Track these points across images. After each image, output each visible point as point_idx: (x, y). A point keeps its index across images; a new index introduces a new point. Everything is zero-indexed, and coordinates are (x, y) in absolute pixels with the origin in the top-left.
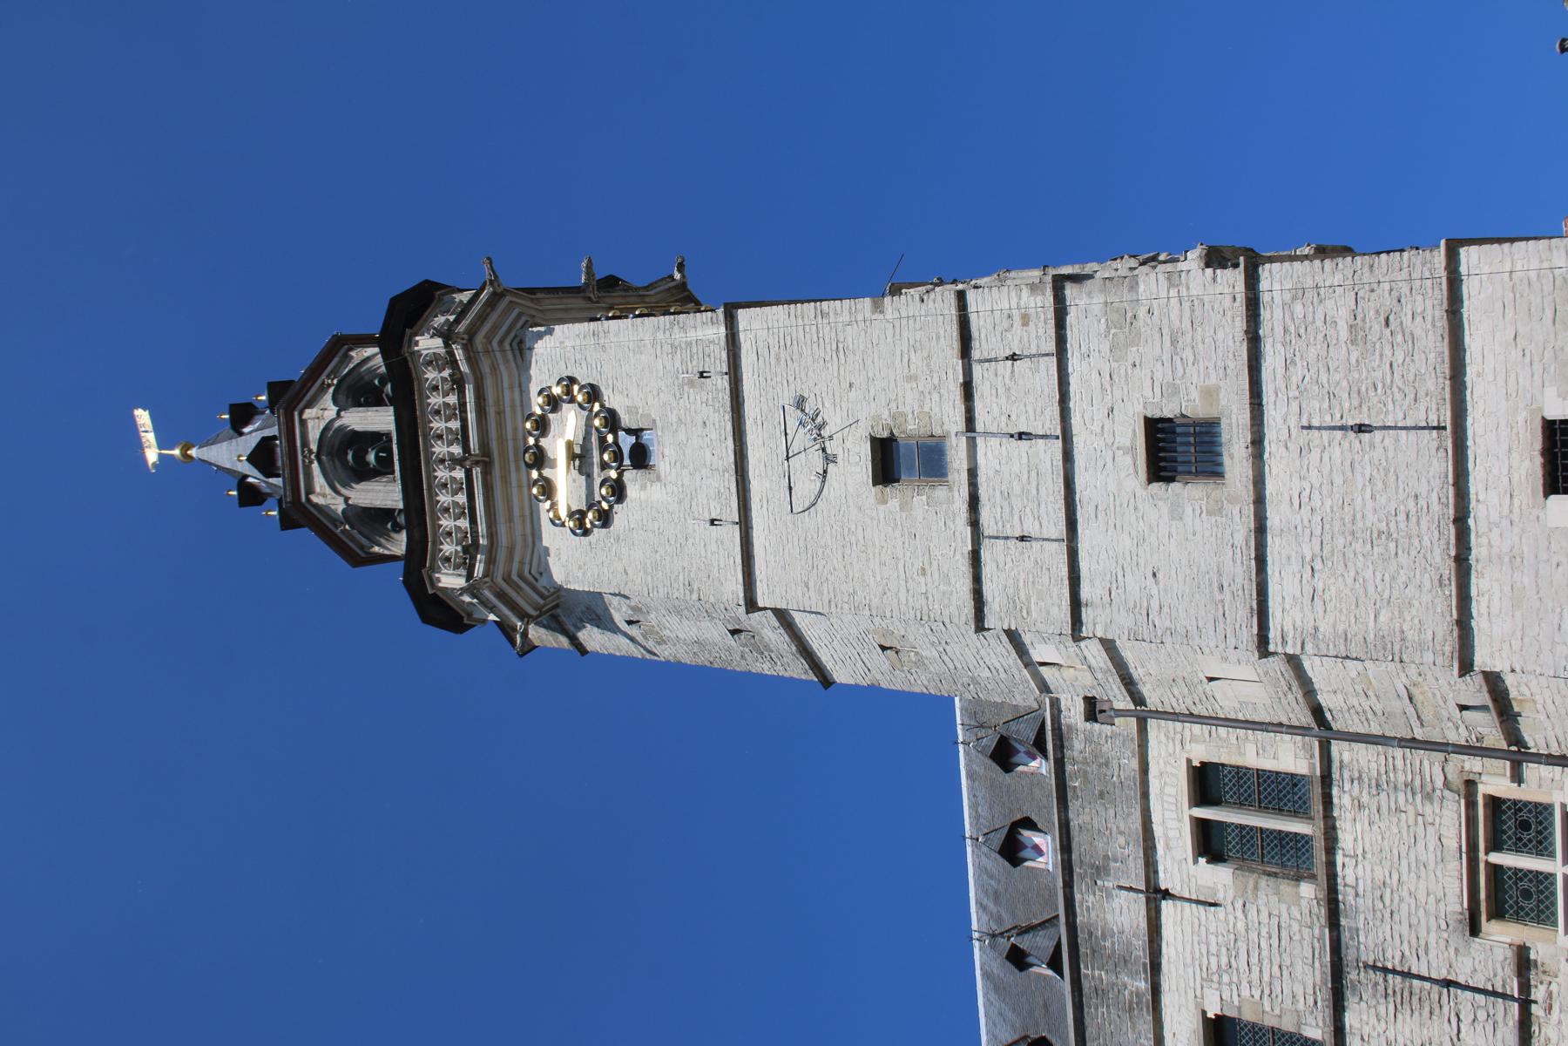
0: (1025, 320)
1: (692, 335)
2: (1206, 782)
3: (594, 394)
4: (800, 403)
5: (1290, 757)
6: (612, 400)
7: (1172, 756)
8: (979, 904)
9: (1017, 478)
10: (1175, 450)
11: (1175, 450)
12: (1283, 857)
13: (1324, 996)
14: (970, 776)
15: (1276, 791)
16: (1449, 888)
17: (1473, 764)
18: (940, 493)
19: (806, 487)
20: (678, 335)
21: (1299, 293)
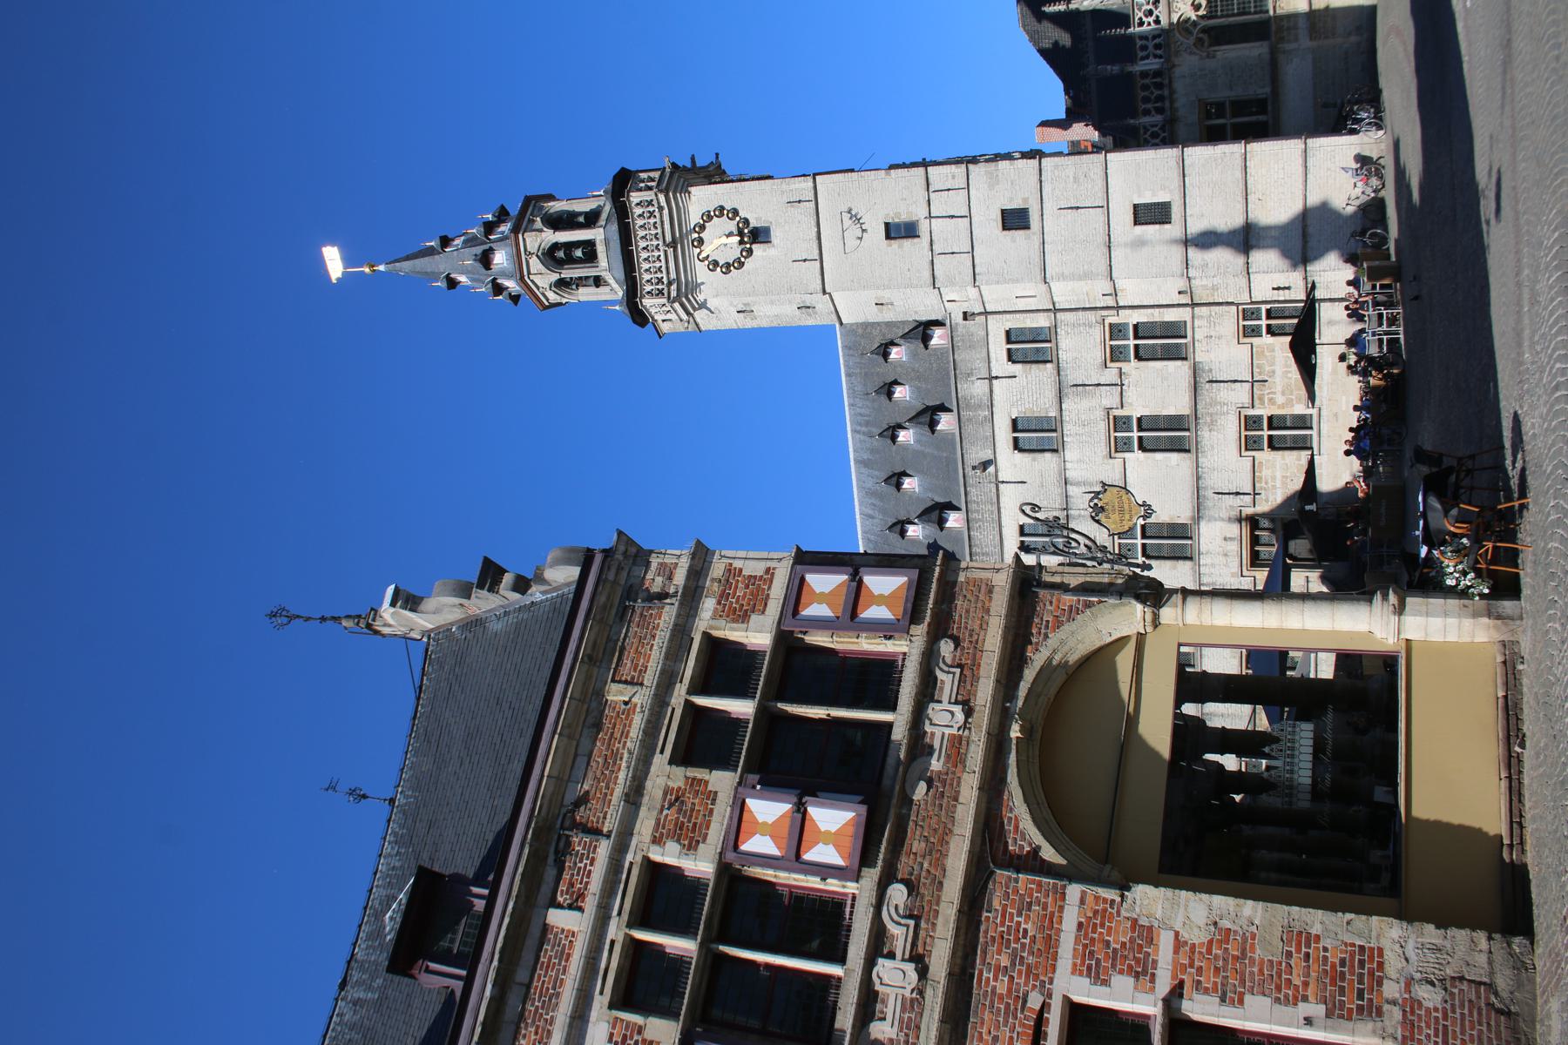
2: (1009, 336)
3: (735, 212)
5: (1042, 321)
6: (742, 214)
7: (997, 327)
8: (854, 431)
9: (947, 234)
10: (1014, 220)
11: (1014, 220)
12: (1039, 359)
13: (1055, 401)
14: (848, 375)
15: (1036, 336)
16: (1097, 354)
17: (1105, 313)
19: (851, 242)
21: (1056, 167)
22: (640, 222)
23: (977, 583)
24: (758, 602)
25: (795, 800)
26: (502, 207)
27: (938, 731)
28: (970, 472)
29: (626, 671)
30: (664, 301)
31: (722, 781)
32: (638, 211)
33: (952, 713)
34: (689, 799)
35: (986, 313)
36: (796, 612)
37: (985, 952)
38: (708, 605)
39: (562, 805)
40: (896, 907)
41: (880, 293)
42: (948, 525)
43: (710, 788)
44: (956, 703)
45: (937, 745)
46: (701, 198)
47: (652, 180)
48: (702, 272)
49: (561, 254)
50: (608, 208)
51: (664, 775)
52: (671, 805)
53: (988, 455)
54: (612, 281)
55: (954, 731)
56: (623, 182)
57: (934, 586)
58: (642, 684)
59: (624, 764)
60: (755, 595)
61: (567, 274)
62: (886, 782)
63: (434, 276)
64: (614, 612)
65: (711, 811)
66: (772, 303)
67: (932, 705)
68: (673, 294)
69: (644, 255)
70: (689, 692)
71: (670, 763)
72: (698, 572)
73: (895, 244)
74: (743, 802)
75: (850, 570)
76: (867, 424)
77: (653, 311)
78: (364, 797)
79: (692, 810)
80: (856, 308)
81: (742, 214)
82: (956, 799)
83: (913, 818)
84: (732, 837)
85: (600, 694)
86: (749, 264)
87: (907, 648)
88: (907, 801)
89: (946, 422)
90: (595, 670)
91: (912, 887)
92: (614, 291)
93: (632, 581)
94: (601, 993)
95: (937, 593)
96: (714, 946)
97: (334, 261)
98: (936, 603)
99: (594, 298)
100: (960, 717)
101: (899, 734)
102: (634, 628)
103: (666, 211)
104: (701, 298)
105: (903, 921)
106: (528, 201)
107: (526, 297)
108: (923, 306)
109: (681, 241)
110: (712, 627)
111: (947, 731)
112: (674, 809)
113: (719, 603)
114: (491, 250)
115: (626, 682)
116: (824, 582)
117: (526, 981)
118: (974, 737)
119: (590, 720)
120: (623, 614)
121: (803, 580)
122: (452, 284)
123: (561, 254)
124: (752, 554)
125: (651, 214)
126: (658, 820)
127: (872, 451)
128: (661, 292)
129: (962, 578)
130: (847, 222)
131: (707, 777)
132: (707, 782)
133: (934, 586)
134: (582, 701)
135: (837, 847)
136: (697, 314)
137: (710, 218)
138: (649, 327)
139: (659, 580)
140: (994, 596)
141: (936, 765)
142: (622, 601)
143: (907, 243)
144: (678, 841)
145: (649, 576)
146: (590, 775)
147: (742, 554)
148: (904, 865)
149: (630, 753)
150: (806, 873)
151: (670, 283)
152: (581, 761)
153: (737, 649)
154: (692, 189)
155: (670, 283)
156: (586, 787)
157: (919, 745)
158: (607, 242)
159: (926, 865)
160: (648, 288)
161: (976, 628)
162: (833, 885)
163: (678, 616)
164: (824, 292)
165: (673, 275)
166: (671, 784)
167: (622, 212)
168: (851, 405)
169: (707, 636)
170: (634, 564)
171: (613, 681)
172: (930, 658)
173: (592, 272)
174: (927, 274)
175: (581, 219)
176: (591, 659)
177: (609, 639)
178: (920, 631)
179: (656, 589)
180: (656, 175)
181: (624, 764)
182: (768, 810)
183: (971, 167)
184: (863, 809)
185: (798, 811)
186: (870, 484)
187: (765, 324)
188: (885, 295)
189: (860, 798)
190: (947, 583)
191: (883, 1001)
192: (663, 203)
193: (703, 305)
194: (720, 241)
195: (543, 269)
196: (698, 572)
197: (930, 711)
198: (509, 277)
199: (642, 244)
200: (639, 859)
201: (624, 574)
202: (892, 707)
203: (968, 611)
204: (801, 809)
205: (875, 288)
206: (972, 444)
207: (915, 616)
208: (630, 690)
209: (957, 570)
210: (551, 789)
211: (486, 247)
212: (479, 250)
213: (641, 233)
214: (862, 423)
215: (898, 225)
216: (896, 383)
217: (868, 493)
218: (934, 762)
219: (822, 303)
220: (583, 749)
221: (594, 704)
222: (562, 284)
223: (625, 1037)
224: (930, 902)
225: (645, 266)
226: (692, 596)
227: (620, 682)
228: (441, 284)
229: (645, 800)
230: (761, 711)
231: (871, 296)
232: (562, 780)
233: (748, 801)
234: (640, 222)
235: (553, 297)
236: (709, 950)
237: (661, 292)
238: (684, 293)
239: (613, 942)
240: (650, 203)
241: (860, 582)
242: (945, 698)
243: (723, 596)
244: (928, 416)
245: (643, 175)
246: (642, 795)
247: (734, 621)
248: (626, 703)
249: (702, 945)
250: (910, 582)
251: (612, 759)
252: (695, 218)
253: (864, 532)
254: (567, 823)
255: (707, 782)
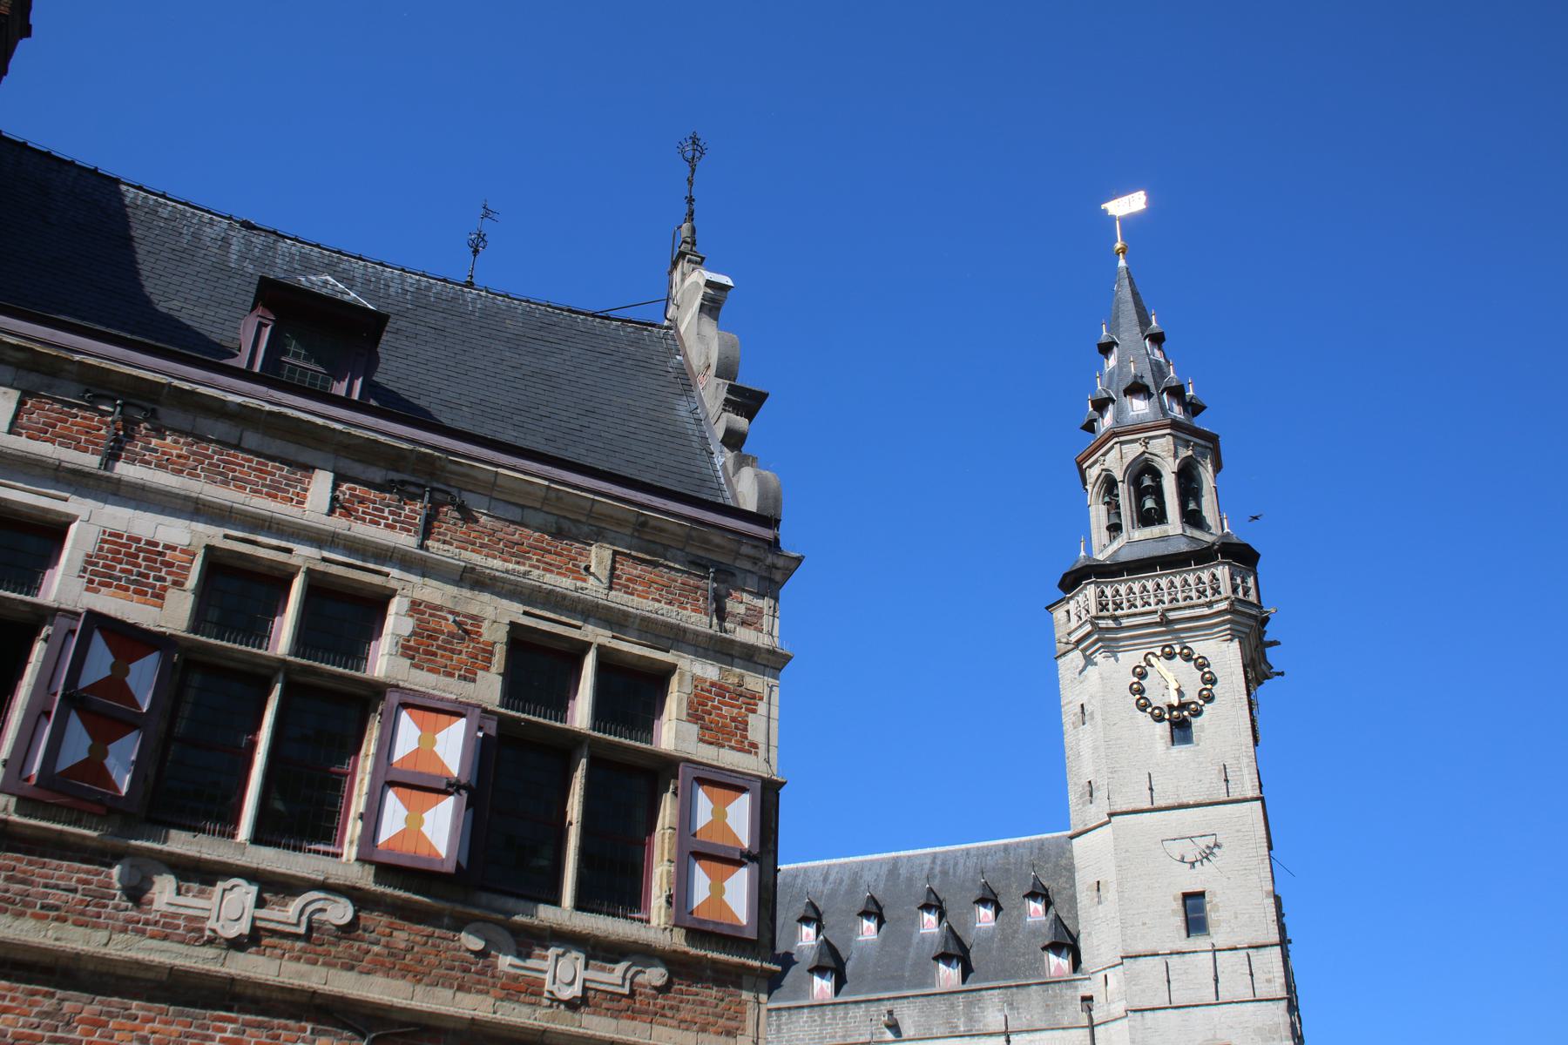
0: (1269, 981)
1: (1246, 771)
3: (1209, 699)
4: (1217, 845)
6: (1207, 708)
8: (935, 856)
9: (1193, 975)
14: (1006, 847)
18: (1183, 933)
19: (1177, 849)
20: (1245, 761)
22: (1191, 579)
23: (739, 1015)
24: (714, 734)
25: (464, 781)
26: (1203, 408)
27: (547, 965)
28: (887, 1006)
29: (627, 569)
30: (1093, 612)
31: (488, 688)
32: (1206, 576)
33: (571, 983)
34: (466, 648)
35: (1092, 1027)
36: (701, 781)
37: (259, 1026)
38: (710, 671)
39: (461, 489)
40: (322, 910)
41: (1113, 888)
42: (816, 979)
43: (480, 673)
44: (585, 989)
45: (530, 963)
46: (1225, 656)
47: (1246, 593)
48: (1131, 658)
49: (1147, 481)
50: (1208, 538)
51: (498, 616)
52: (458, 624)
53: (908, 1029)
54: (1115, 546)
55: (548, 986)
56: (1242, 556)
57: (736, 959)
58: (610, 588)
59: (511, 566)
60: (722, 729)
61: (1124, 492)
62: (484, 898)
63: (1114, 327)
64: (701, 553)
65: (452, 675)
66: (1095, 749)
67: (582, 957)
68: (1103, 624)
69: (1150, 585)
70: (600, 648)
71: (512, 624)
72: (750, 657)
73: (1178, 905)
74: (461, 715)
75: (756, 851)
76: (944, 873)
77: (1080, 598)
78: (476, 252)
79: (453, 651)
80: (1093, 856)
81: (1207, 708)
82: (460, 988)
83: (438, 932)
84: (418, 701)
85: (599, 536)
86: (1144, 718)
87: (655, 924)
88: (459, 924)
89: (948, 975)
90: (628, 531)
91: (348, 930)
92: (1103, 549)
93: (740, 576)
94: (226, 537)
95: (727, 963)
96: (281, 677)
97: (1128, 205)
98: (714, 962)
99: (1093, 520)
100: (567, 994)
101: (546, 914)
102: (680, 578)
103: (1206, 611)
104: (1099, 658)
105: (304, 919)
106: (1213, 439)
107: (1091, 440)
108: (1098, 943)
109: (1170, 632)
110: (682, 675)
111: (548, 977)
112: (455, 629)
113: (713, 684)
114: (1149, 395)
115: (613, 568)
116: (739, 816)
117: (244, 445)
118: (540, 1012)
119: (566, 525)
120: (698, 565)
121: (742, 790)
122: (1106, 349)
123: (1147, 481)
124: (774, 725)
125: (1202, 593)
126: (440, 608)
127: (910, 880)
128: (1104, 607)
129: (746, 995)
130: (1203, 843)
131: (494, 669)
132: (487, 669)
133: (736, 959)
134: (590, 514)
135: (403, 833)
136: (1077, 654)
137: (1200, 667)
138: (1061, 594)
139: (741, 609)
140: (723, 1039)
141: (505, 962)
142: (714, 563)
143: (1179, 921)
144: (414, 633)
145: (746, 597)
146: (499, 524)
147: (775, 712)
148: (377, 921)
149: (526, 574)
150: (371, 794)
151: (1115, 618)
152: (515, 513)
153: (654, 707)
154: (1236, 644)
155: (1115, 618)
156: (483, 519)
157: (530, 940)
158: (1164, 538)
159: (376, 949)
160: (1109, 591)
161: (682, 1015)
162: (354, 829)
163: (697, 634)
164: (1111, 815)
165: (1125, 622)
166: (486, 624)
167: (1203, 556)
168: (968, 852)
169: (671, 669)
170: (761, 578)
171: (615, 553)
172: (643, 954)
173: (1126, 520)
174: (1140, 948)
175: (1192, 506)
176: (642, 525)
177: (667, 547)
178: (677, 941)
179: (731, 605)
180: (1252, 598)
181: (511, 566)
182: (451, 747)
183: (1284, 1004)
184: (450, 868)
185: (450, 785)
186: (868, 877)
187: (1069, 739)
188: (1110, 894)
189: (464, 863)
190: (739, 976)
191: (201, 892)
192: (1216, 608)
193: (1089, 661)
194: (1171, 680)
195: (1127, 461)
196: (750, 657)
197: (574, 954)
198: (1117, 419)
199: (1164, 583)
200: (393, 584)
201: (748, 566)
202: (581, 905)
203: (703, 1003)
204: (451, 788)
205: (1119, 879)
206: (921, 1010)
207: (698, 934)
208: (604, 574)
209: (756, 989)
210: (481, 476)
211: (1153, 389)
212: (1149, 380)
213: (1178, 581)
214: (945, 866)
215: (1201, 909)
216: (998, 909)
217: (856, 875)
218: (509, 959)
219: (1097, 812)
220: (530, 516)
221: (586, 529)
222: (1110, 484)
223: (170, 565)
224: (328, 953)
225: (1136, 587)
226: (721, 650)
227: (614, 561)
228: (1105, 336)
229: (466, 593)
230: (577, 738)
231: (1109, 877)
232: (492, 489)
233: (463, 721)
234: (1191, 579)
235: (1093, 473)
236: (276, 671)
237: (1104, 607)
238: (1104, 636)
239: (289, 551)
240: (1216, 591)
241: (740, 864)
242: (591, 974)
243: (720, 689)
244: (956, 951)
245: (1251, 581)
246: (472, 588)
247: (690, 704)
248: (587, 568)
249: (283, 662)
250: (740, 928)
251: (517, 551)
252: (1199, 648)
253: (806, 870)
254: (438, 496)
255: (487, 669)
